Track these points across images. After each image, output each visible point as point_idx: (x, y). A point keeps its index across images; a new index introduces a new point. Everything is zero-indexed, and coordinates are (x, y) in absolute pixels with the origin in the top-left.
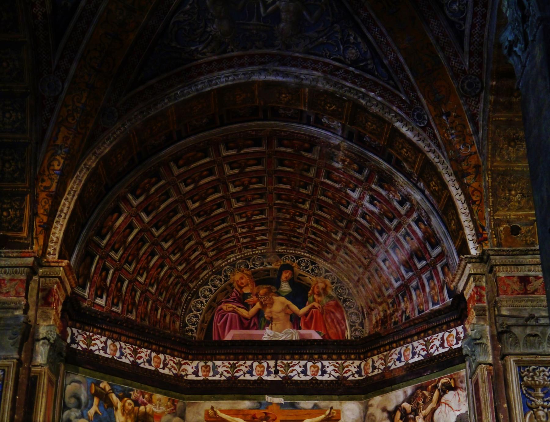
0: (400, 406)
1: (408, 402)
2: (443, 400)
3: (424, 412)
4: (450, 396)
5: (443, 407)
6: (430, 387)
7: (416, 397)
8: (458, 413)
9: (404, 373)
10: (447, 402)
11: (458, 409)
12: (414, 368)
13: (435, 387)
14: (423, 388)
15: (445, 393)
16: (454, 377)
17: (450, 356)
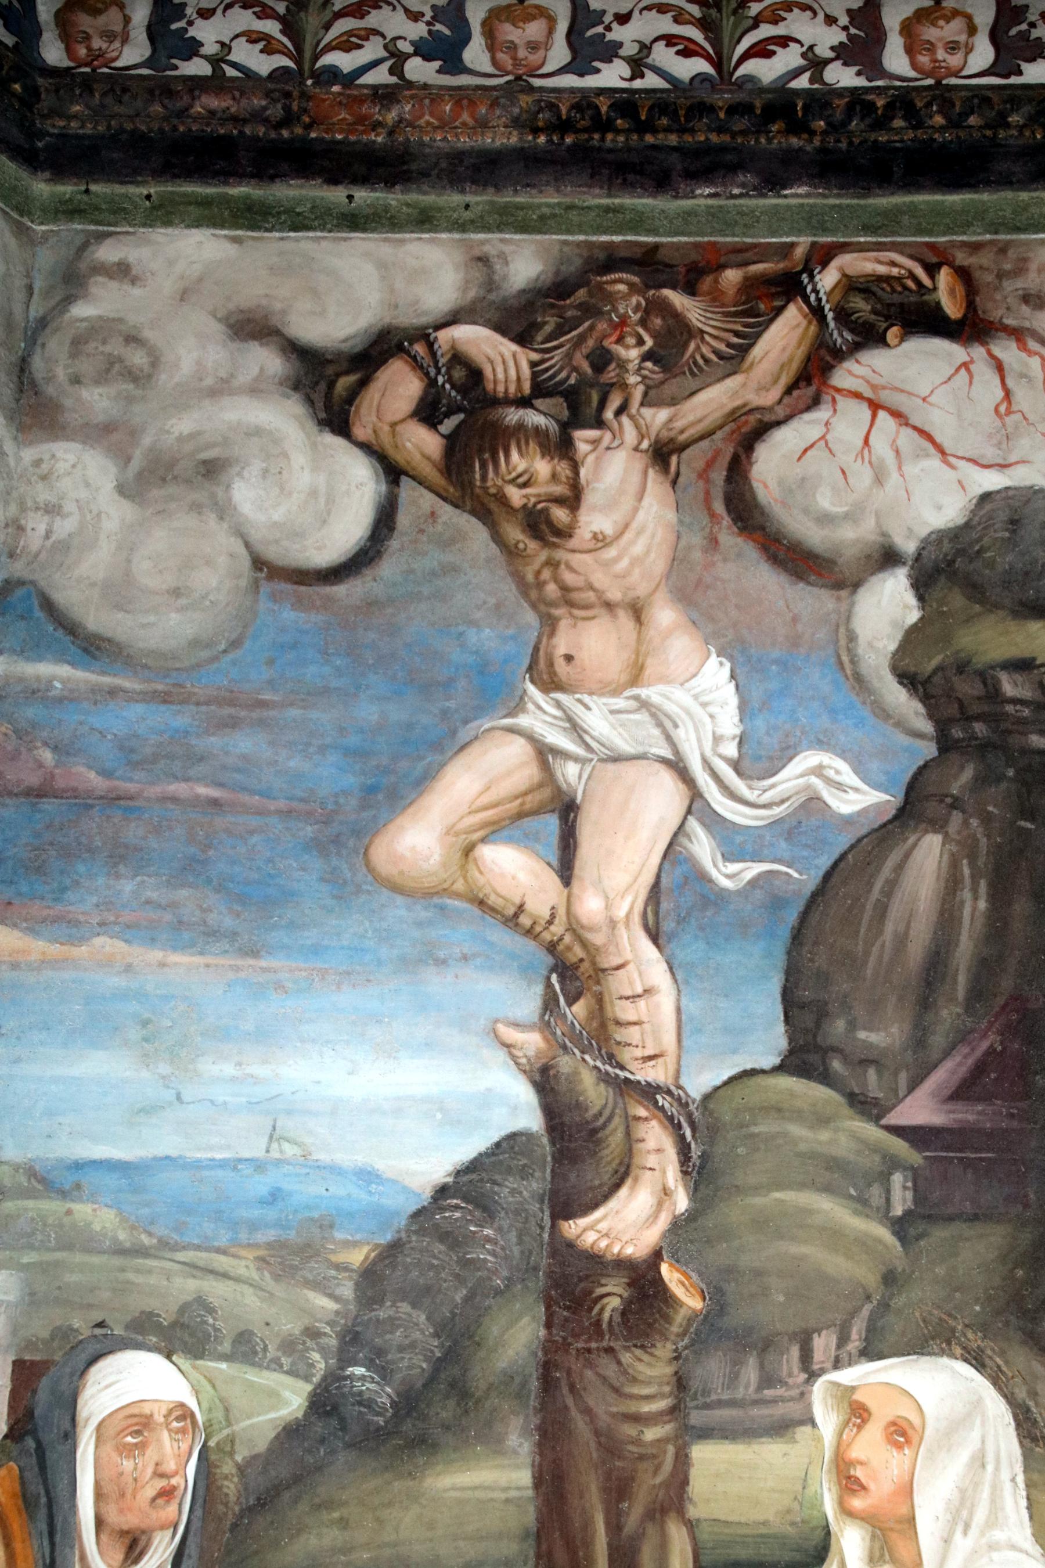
0: (424, 335)
1: (500, 328)
2: (848, 375)
3: (658, 417)
4: (916, 365)
5: (843, 423)
6: (732, 277)
7: (589, 311)
8: (993, 481)
9: (501, 138)
10: (886, 397)
11: (990, 454)
12: (603, 125)
13: (789, 286)
14: (650, 266)
15: (869, 337)
16: (961, 258)
17: (955, 123)
